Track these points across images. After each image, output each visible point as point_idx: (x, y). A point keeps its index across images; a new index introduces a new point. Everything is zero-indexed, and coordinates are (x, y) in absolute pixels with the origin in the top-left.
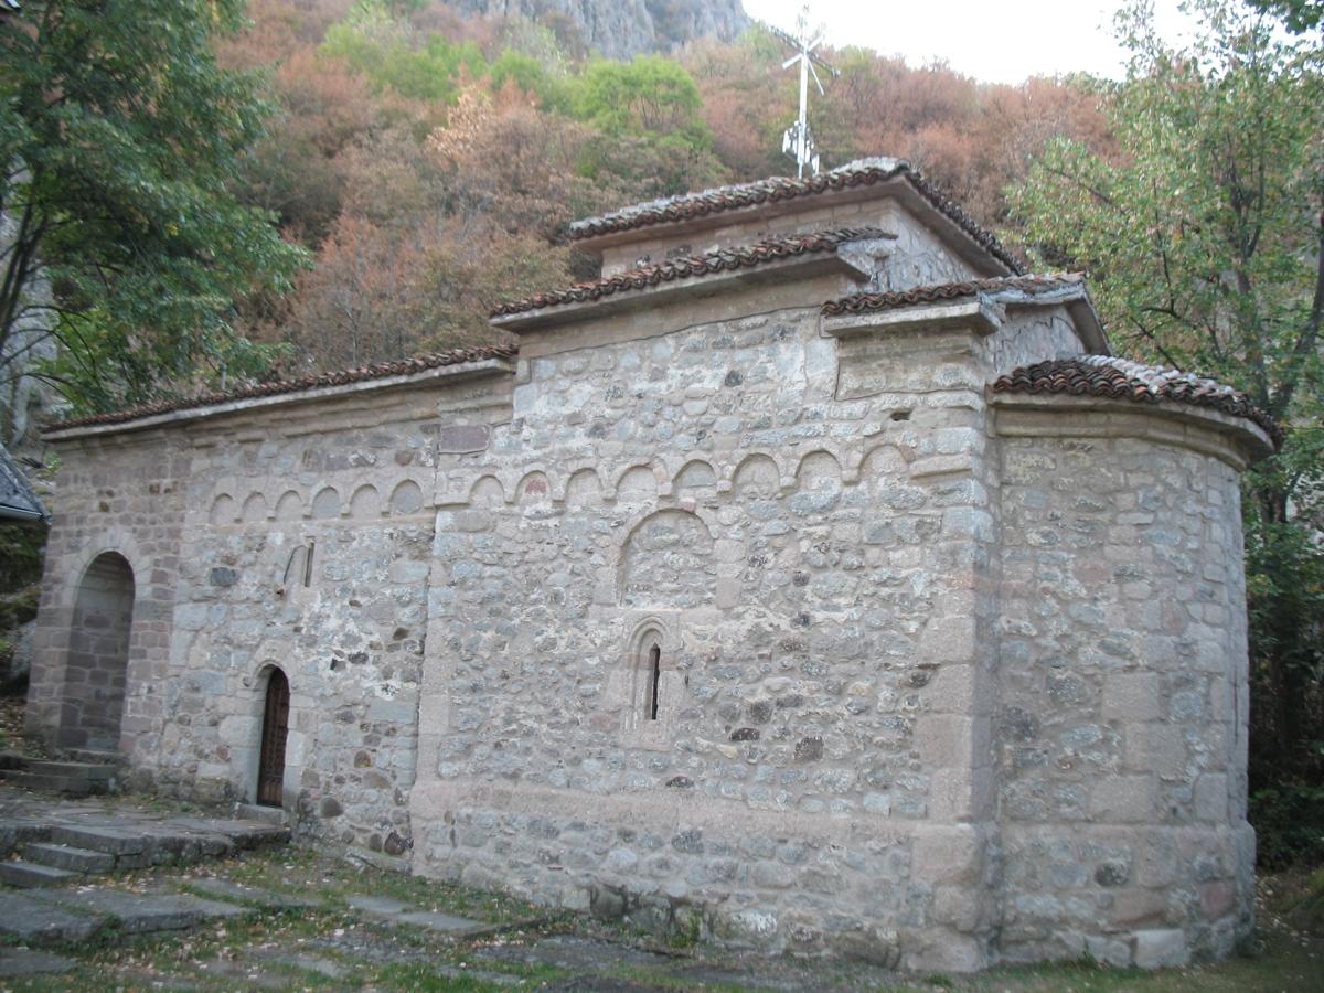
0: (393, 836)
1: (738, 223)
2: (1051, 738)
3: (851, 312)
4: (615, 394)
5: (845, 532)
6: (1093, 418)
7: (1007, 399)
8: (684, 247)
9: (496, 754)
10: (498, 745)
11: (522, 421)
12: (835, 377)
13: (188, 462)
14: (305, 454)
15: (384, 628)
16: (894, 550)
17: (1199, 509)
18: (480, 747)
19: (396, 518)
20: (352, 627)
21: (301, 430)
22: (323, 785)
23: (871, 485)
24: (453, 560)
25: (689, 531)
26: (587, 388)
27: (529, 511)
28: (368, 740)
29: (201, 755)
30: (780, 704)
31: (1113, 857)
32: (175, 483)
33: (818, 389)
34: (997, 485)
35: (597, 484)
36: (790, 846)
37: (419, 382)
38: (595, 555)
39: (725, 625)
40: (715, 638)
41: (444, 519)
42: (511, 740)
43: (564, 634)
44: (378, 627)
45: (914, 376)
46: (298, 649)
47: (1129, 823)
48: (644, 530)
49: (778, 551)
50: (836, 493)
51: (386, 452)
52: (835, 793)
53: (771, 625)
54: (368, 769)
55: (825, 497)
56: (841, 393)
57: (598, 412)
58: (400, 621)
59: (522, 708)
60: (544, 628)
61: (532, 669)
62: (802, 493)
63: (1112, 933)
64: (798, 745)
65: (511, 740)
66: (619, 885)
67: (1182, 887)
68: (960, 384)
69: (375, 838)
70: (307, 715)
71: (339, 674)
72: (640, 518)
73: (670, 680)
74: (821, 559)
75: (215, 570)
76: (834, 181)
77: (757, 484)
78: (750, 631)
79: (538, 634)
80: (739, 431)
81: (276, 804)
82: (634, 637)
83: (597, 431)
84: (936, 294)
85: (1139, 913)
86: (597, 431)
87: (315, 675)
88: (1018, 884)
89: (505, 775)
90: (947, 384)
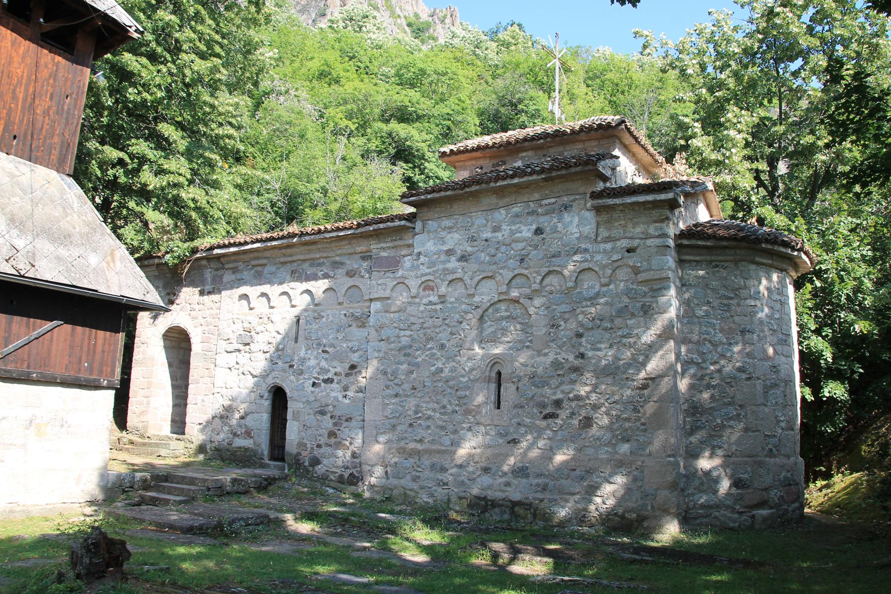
0: (351, 474)
1: (532, 150)
2: (710, 414)
3: (605, 197)
4: (472, 239)
7: (685, 242)
8: (501, 161)
9: (410, 430)
10: (411, 425)
11: (419, 254)
12: (595, 230)
13: (221, 277)
14: (292, 271)
15: (343, 364)
16: (630, 319)
17: (779, 297)
18: (401, 426)
19: (347, 305)
20: (323, 364)
21: (290, 259)
22: (309, 449)
23: (617, 287)
24: (381, 327)
25: (517, 311)
26: (456, 236)
27: (425, 301)
28: (335, 424)
29: (235, 435)
31: (743, 474)
32: (214, 288)
33: (586, 237)
34: (680, 286)
35: (464, 286)
36: (578, 473)
37: (361, 233)
38: (464, 324)
39: (538, 359)
40: (533, 366)
41: (376, 306)
42: (419, 422)
43: (447, 365)
44: (339, 364)
46: (292, 377)
47: (749, 456)
48: (490, 310)
49: (566, 321)
51: (340, 271)
52: (601, 444)
53: (564, 359)
54: (335, 440)
55: (592, 293)
56: (599, 239)
57: (463, 248)
58: (352, 360)
59: (424, 405)
60: (436, 363)
61: (429, 384)
62: (578, 290)
63: (742, 512)
64: (580, 420)
65: (419, 422)
66: (483, 496)
67: (775, 489)
68: (663, 234)
69: (341, 476)
70: (298, 412)
71: (317, 389)
72: (489, 304)
73: (509, 392)
75: (240, 335)
76: (586, 128)
78: (552, 362)
79: (432, 366)
80: (543, 259)
81: (282, 459)
82: (487, 366)
83: (463, 258)
84: (651, 188)
85: (756, 502)
86: (463, 258)
87: (303, 390)
88: (694, 489)
89: (415, 441)
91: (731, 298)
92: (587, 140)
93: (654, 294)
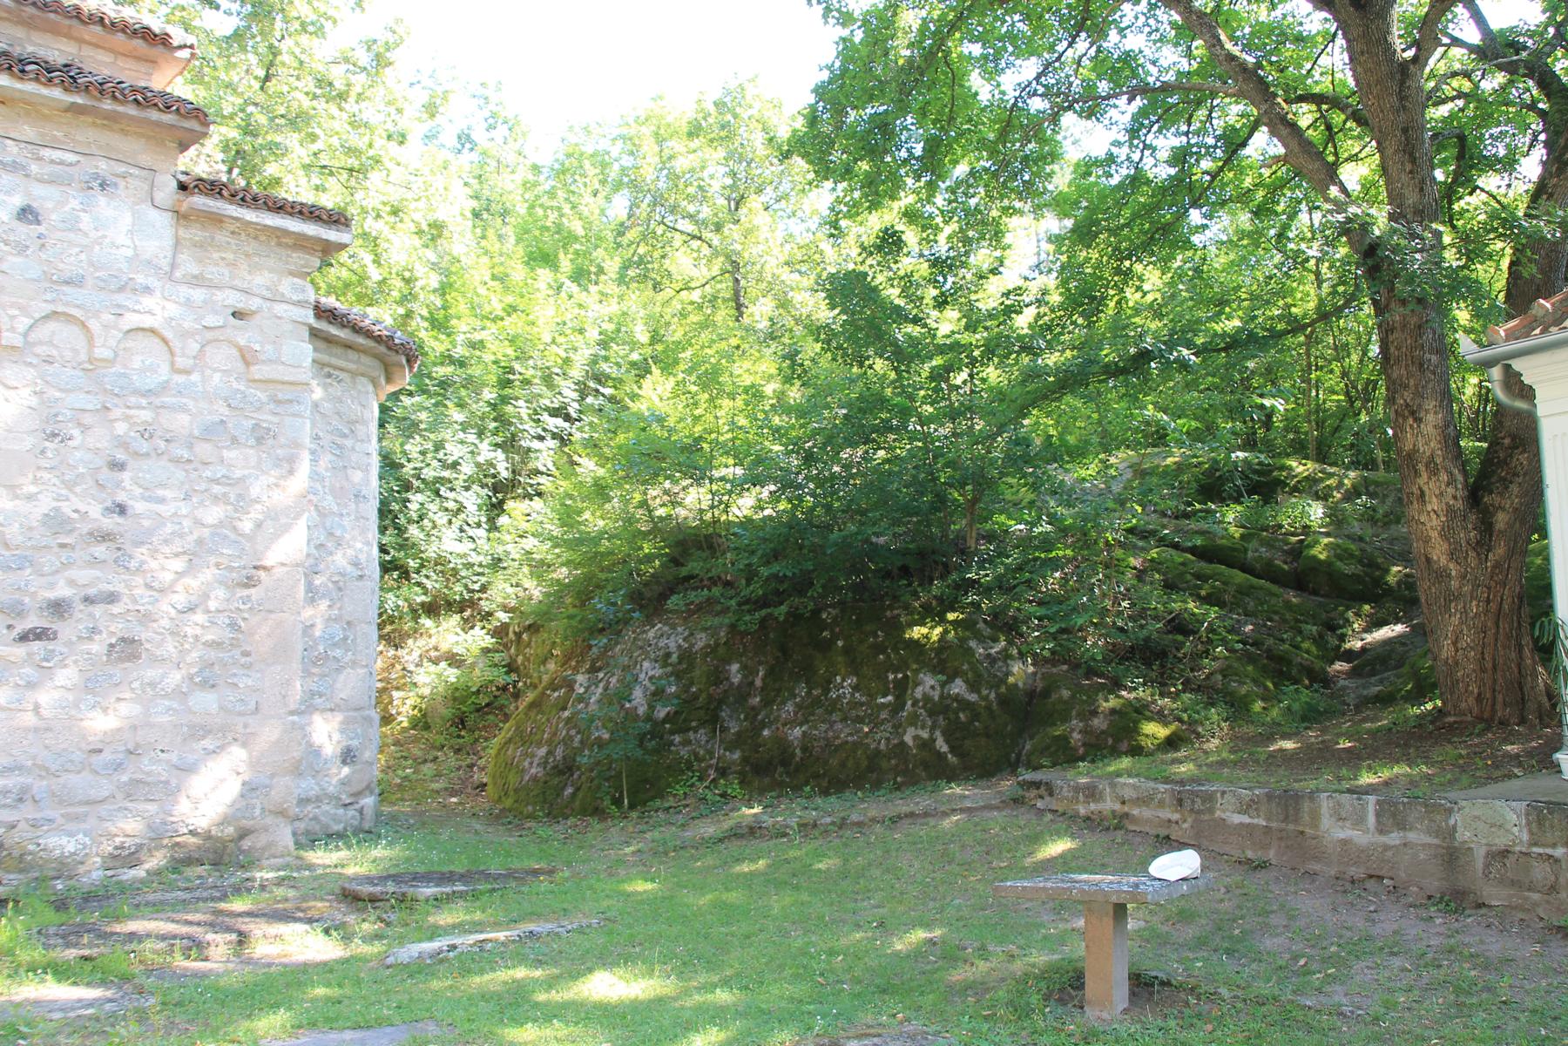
5: (181, 422)
6: (352, 355)
12: (169, 254)
16: (227, 448)
30: (88, 600)
36: (107, 756)
45: (261, 280)
50: (165, 378)
53: (76, 511)
55: (152, 381)
56: (178, 274)
62: (118, 368)
64: (112, 646)
74: (145, 447)
77: (56, 347)
78: (47, 515)
84: (317, 213)
90: (295, 298)
91: (345, 436)
92: (90, 44)
93: (278, 410)
